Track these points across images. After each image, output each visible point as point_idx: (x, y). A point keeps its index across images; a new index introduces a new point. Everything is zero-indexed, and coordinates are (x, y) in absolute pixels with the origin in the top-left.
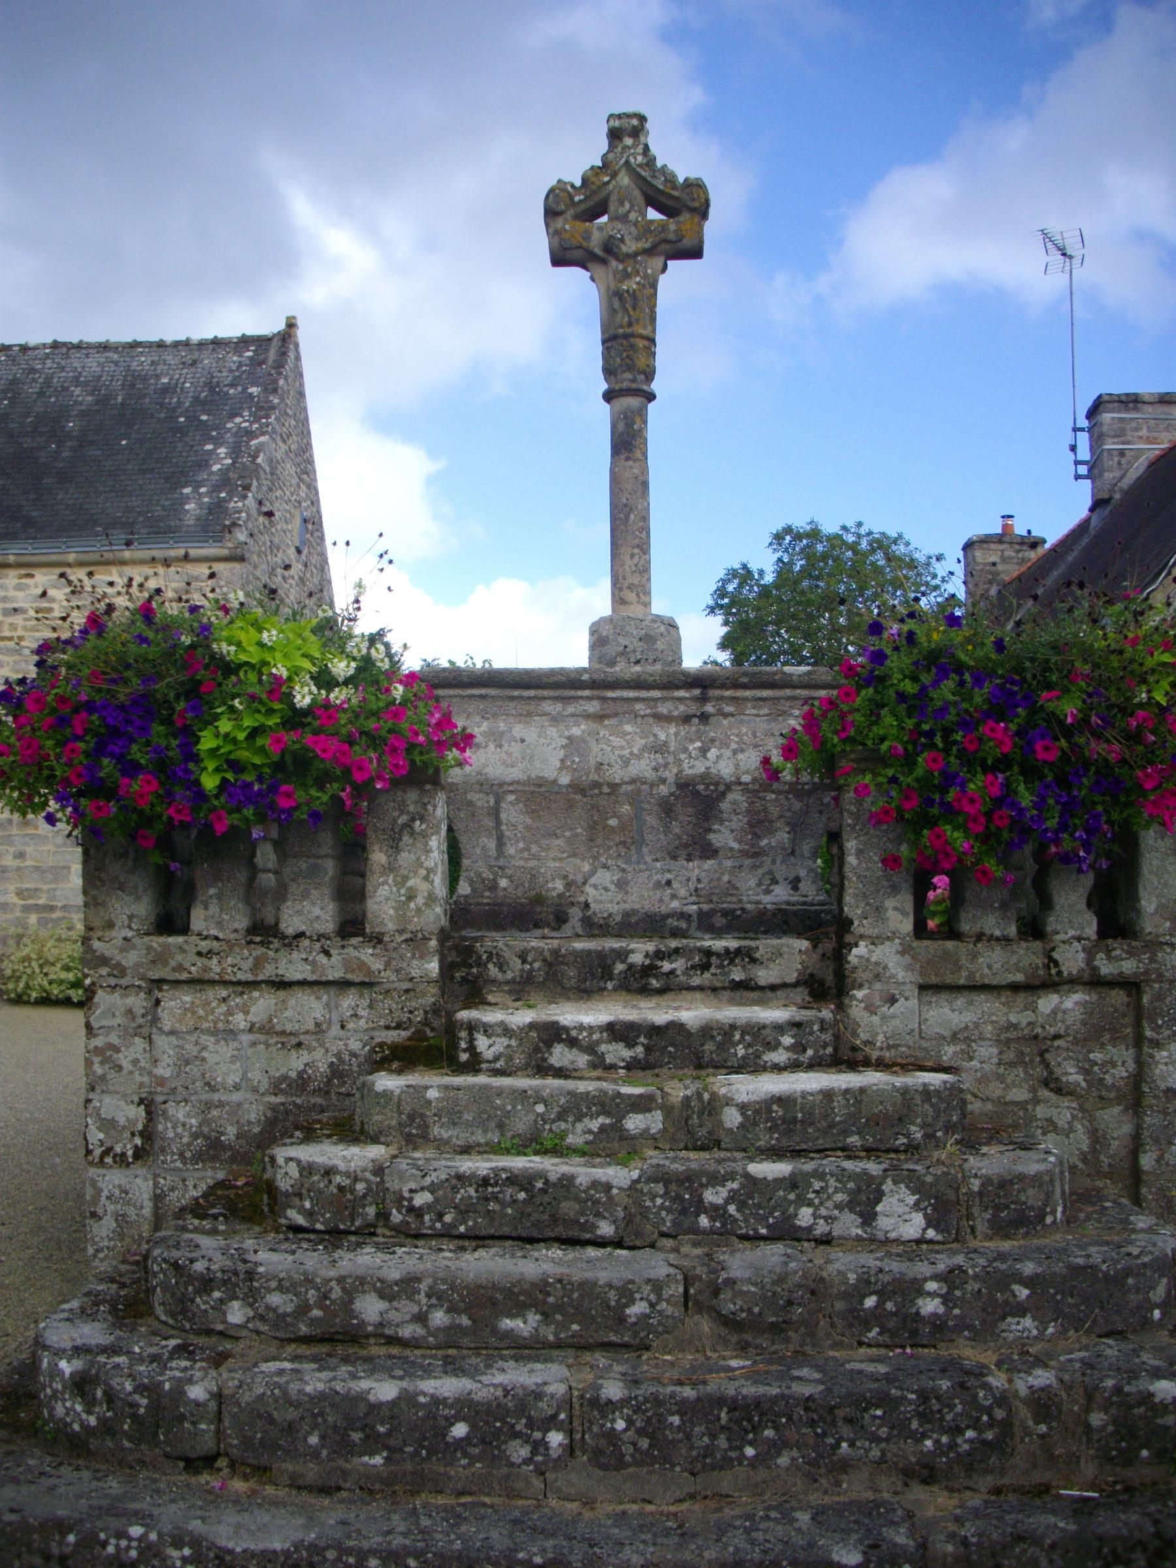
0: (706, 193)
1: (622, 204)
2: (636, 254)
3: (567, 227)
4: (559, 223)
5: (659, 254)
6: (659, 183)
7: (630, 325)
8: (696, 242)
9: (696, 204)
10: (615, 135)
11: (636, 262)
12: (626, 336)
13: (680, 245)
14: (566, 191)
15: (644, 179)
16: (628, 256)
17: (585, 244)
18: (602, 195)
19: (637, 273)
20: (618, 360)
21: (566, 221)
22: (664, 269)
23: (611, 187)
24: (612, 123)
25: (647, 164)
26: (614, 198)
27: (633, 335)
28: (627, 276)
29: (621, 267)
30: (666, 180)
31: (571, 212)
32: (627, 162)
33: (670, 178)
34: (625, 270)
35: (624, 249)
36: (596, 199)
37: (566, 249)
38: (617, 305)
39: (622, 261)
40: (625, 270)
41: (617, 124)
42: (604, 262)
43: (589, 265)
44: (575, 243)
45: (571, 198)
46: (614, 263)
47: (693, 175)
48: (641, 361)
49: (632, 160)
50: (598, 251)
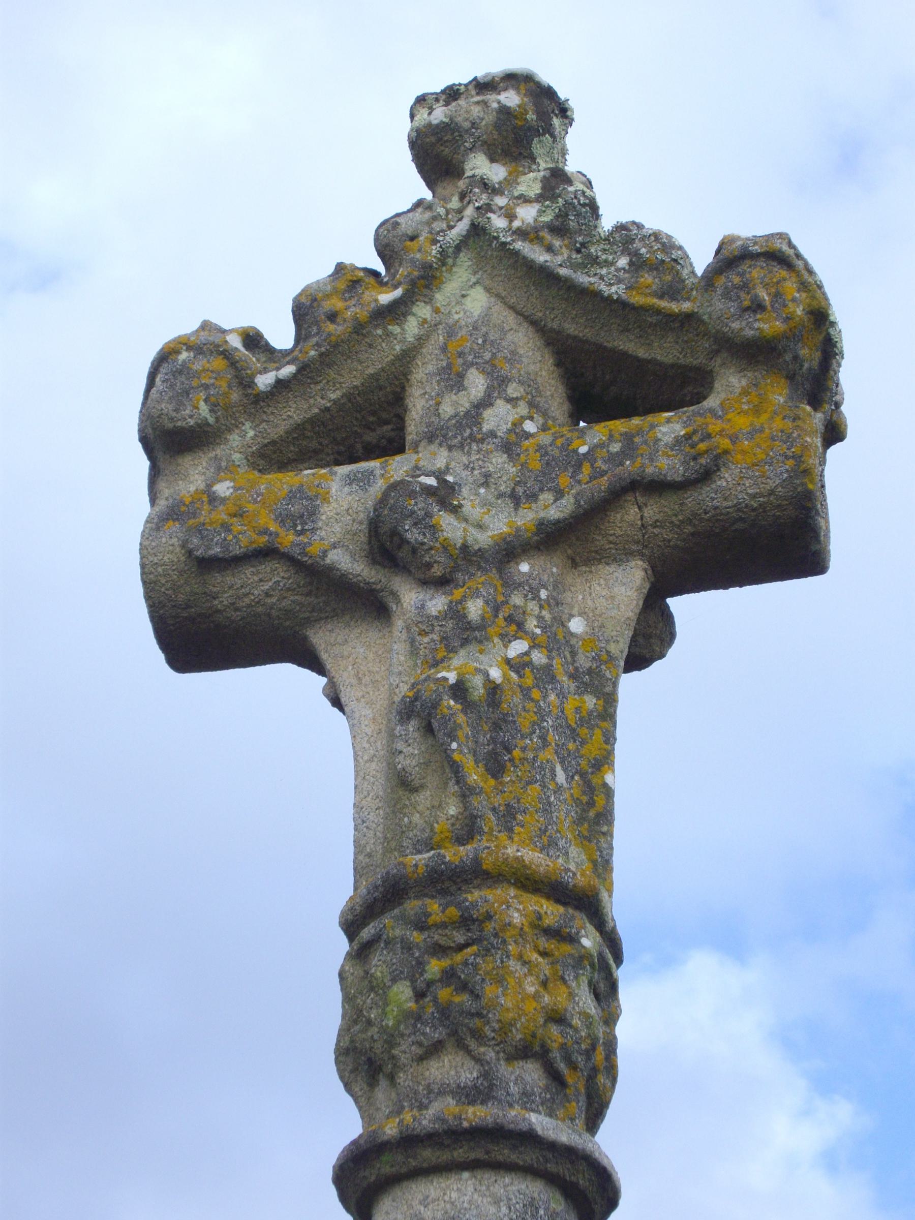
0: (809, 285)
1: (454, 380)
2: (509, 551)
3: (223, 489)
4: (192, 476)
5: (620, 554)
6: (610, 281)
7: (468, 829)
8: (775, 477)
9: (769, 326)
10: (435, 153)
11: (510, 585)
12: (445, 881)
13: (708, 497)
14: (226, 354)
15: (544, 277)
16: (468, 557)
17: (288, 539)
18: (376, 360)
19: (517, 624)
20: (402, 993)
21: (224, 470)
22: (650, 640)
23: (412, 328)
24: (423, 116)
25: (559, 229)
26: (424, 371)
27: (477, 874)
28: (464, 633)
29: (437, 604)
30: (638, 264)
31: (243, 438)
32: (477, 231)
33: (650, 254)
34: (456, 613)
35: (451, 528)
36: (348, 379)
37: (207, 565)
38: (412, 753)
39: (443, 583)
40: (456, 613)
41: (439, 114)
42: (374, 606)
43: (321, 638)
44: (244, 538)
45: (245, 382)
46: (410, 598)
47: (751, 227)
48: (519, 990)
49: (498, 222)
50: (347, 561)
